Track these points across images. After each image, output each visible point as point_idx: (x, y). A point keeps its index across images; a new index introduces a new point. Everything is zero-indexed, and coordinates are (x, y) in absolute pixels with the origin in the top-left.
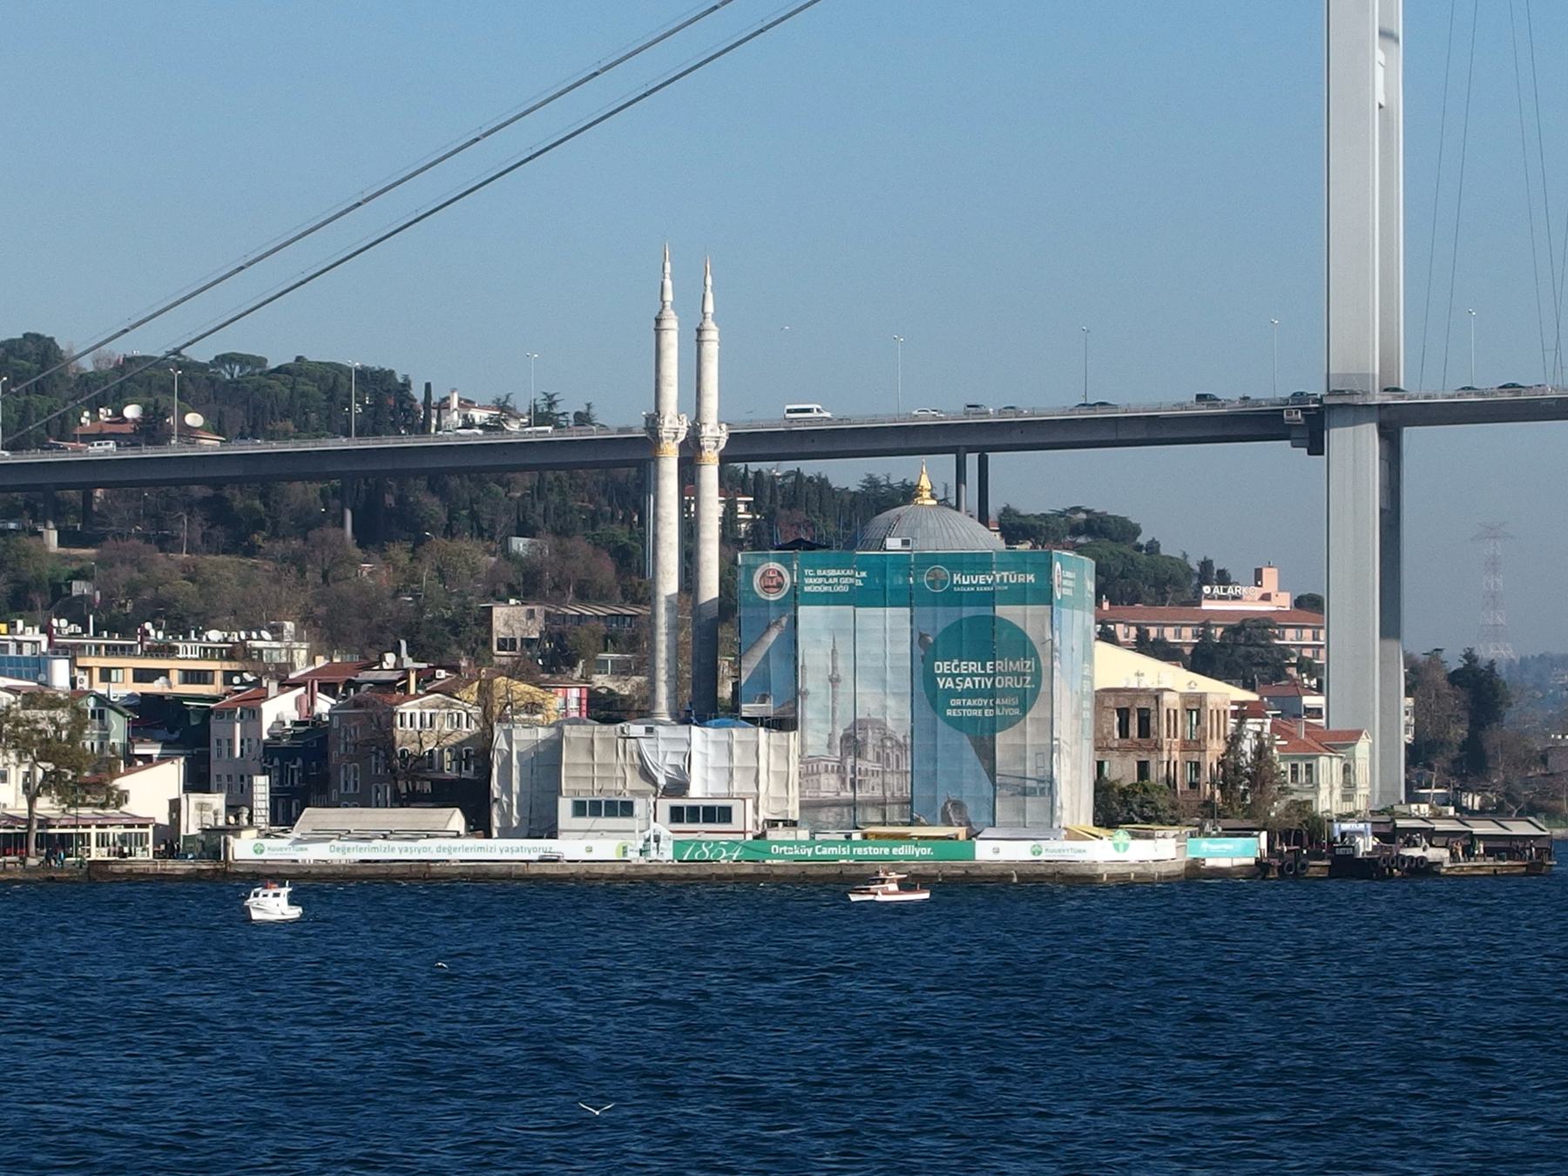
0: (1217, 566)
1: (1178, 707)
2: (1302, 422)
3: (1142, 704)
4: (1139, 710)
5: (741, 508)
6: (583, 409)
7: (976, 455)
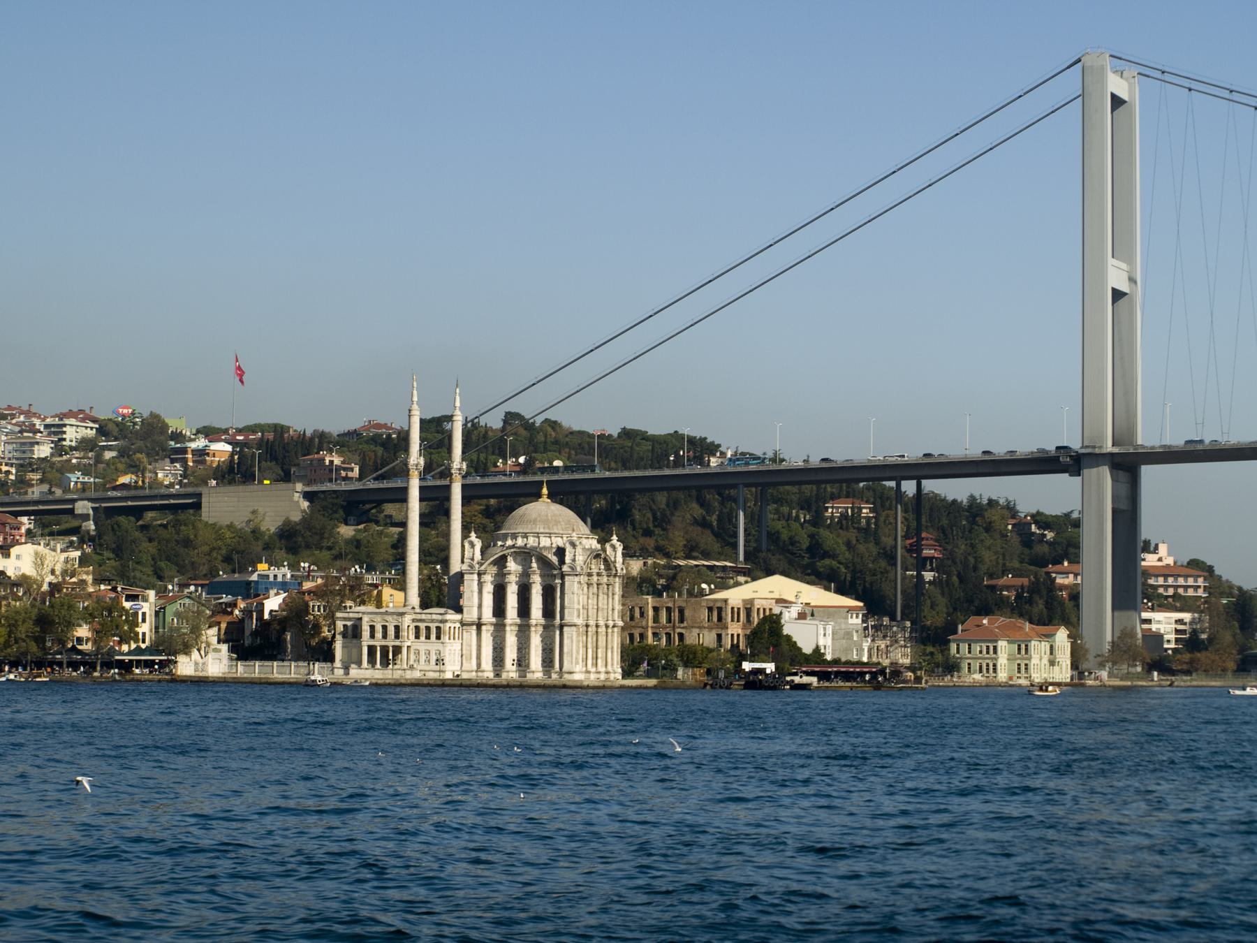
1: (741, 606)
2: (1071, 462)
3: (719, 605)
4: (717, 607)
5: (864, 511)
6: (806, 458)
7: (914, 482)
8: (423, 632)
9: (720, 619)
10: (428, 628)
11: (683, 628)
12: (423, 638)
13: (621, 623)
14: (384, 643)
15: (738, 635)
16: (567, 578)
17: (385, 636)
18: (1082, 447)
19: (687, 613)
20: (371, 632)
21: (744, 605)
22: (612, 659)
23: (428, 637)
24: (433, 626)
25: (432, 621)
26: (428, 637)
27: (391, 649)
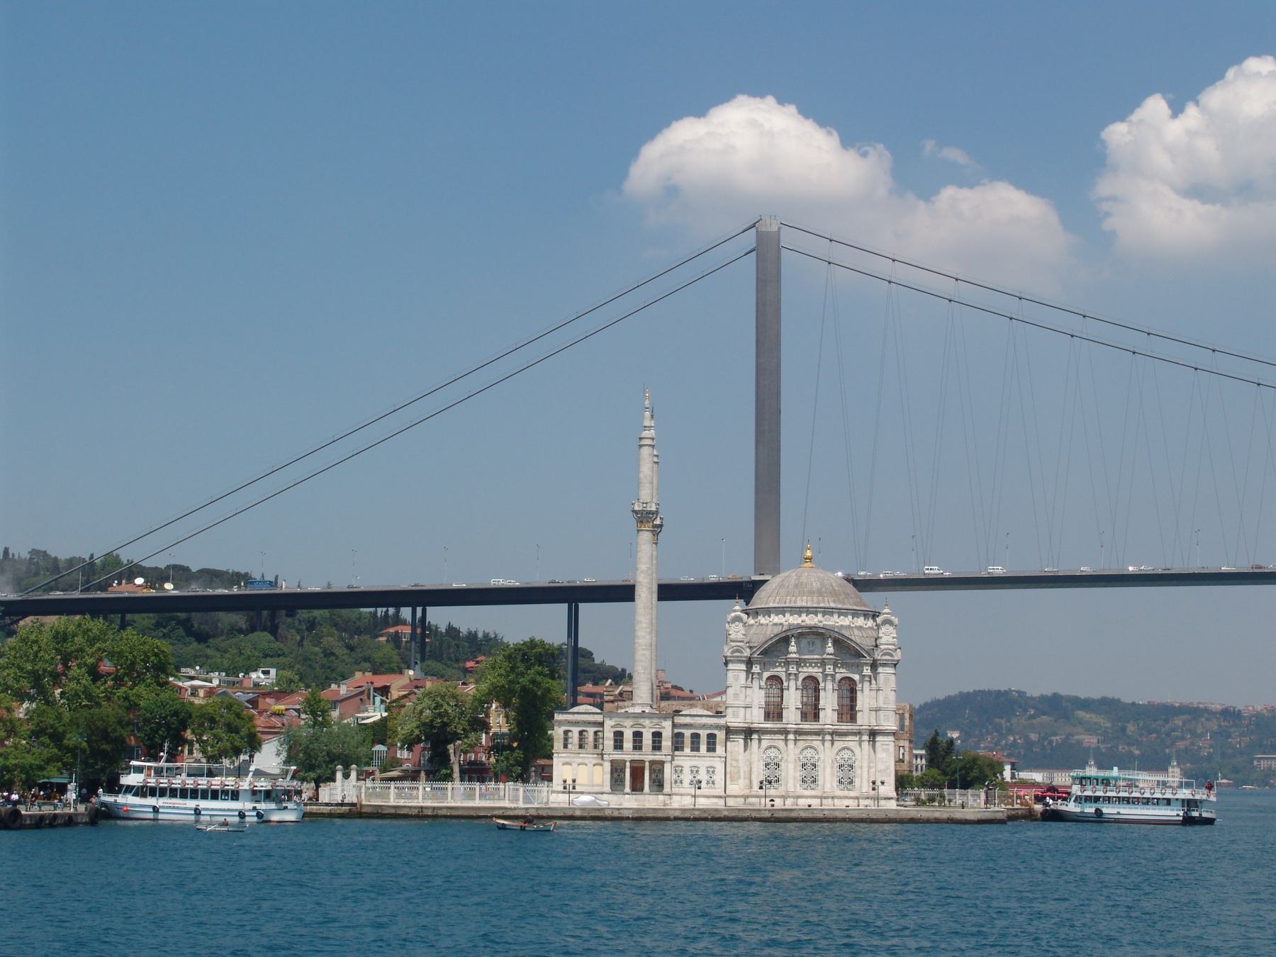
0: (628, 672)
8: (687, 741)
10: (696, 737)
12: (687, 750)
14: (637, 756)
16: (880, 670)
17: (638, 746)
20: (616, 741)
23: (695, 747)
24: (703, 734)
25: (704, 726)
26: (695, 747)
27: (647, 764)
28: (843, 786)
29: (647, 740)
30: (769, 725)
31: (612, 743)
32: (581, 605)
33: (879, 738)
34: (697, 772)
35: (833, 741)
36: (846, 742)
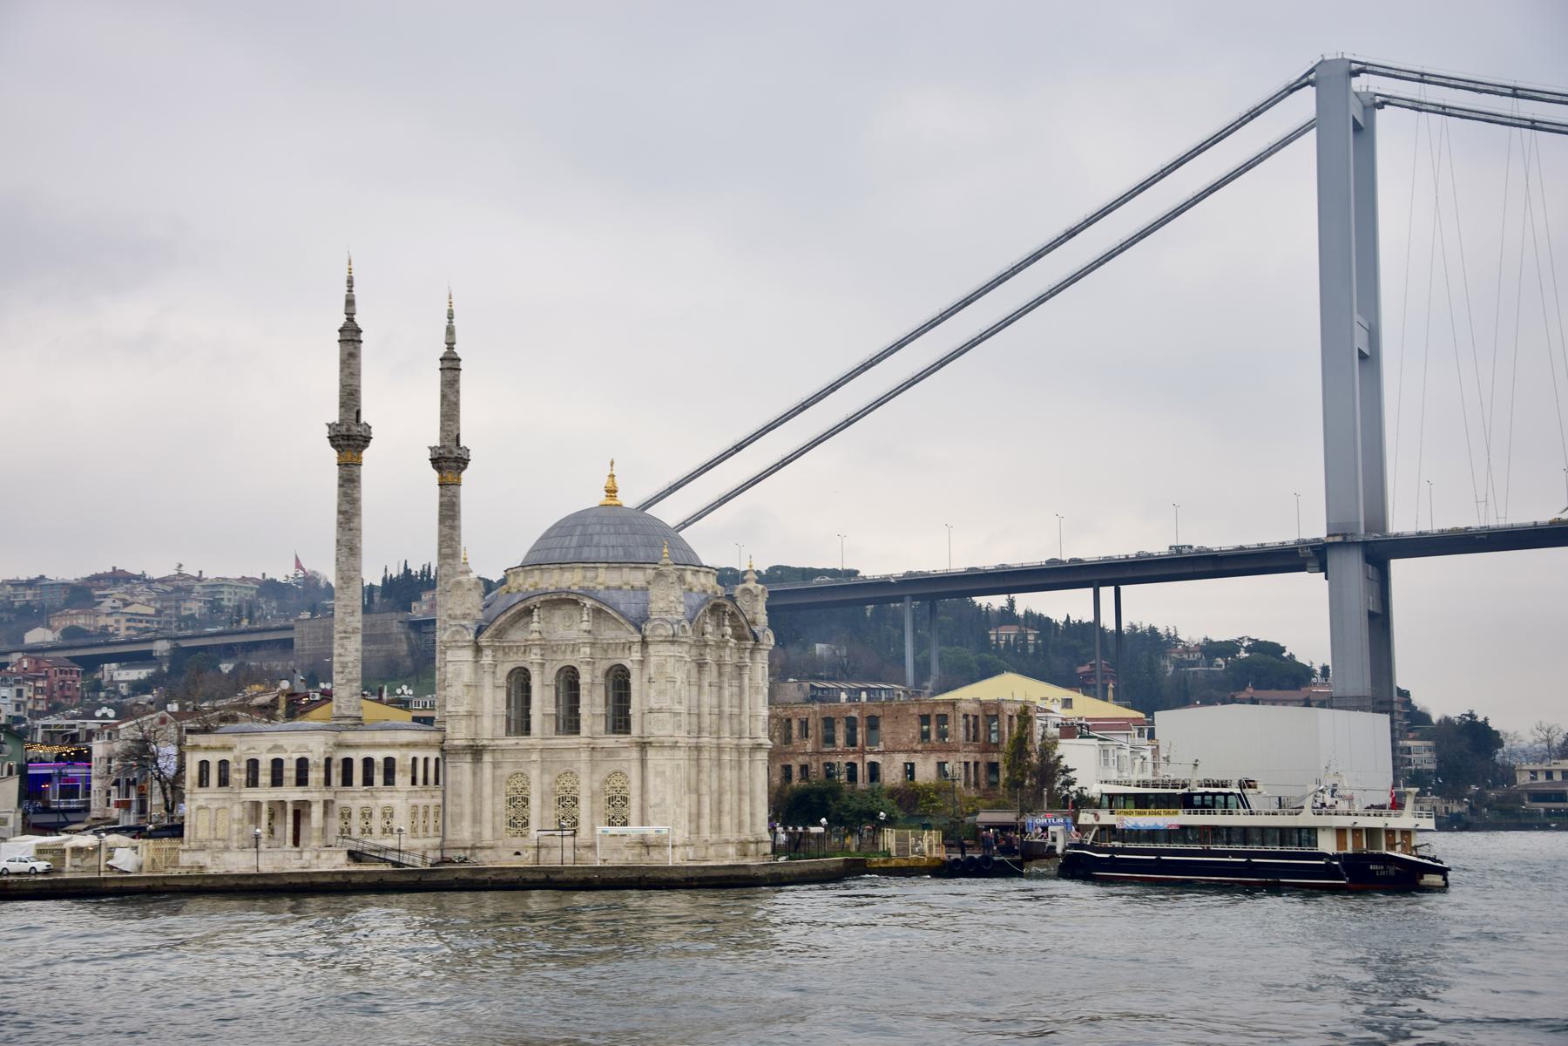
1: (981, 715)
3: (941, 710)
7: (1113, 588)
9: (943, 735)
11: (879, 752)
13: (768, 743)
15: (976, 764)
16: (652, 649)
17: (277, 781)
18: (1328, 536)
19: (884, 727)
21: (984, 711)
22: (752, 815)
28: (514, 830)
29: (290, 772)
30: (511, 741)
31: (244, 777)
32: (1101, 588)
33: (651, 753)
34: (370, 815)
35: (593, 764)
36: (618, 763)
